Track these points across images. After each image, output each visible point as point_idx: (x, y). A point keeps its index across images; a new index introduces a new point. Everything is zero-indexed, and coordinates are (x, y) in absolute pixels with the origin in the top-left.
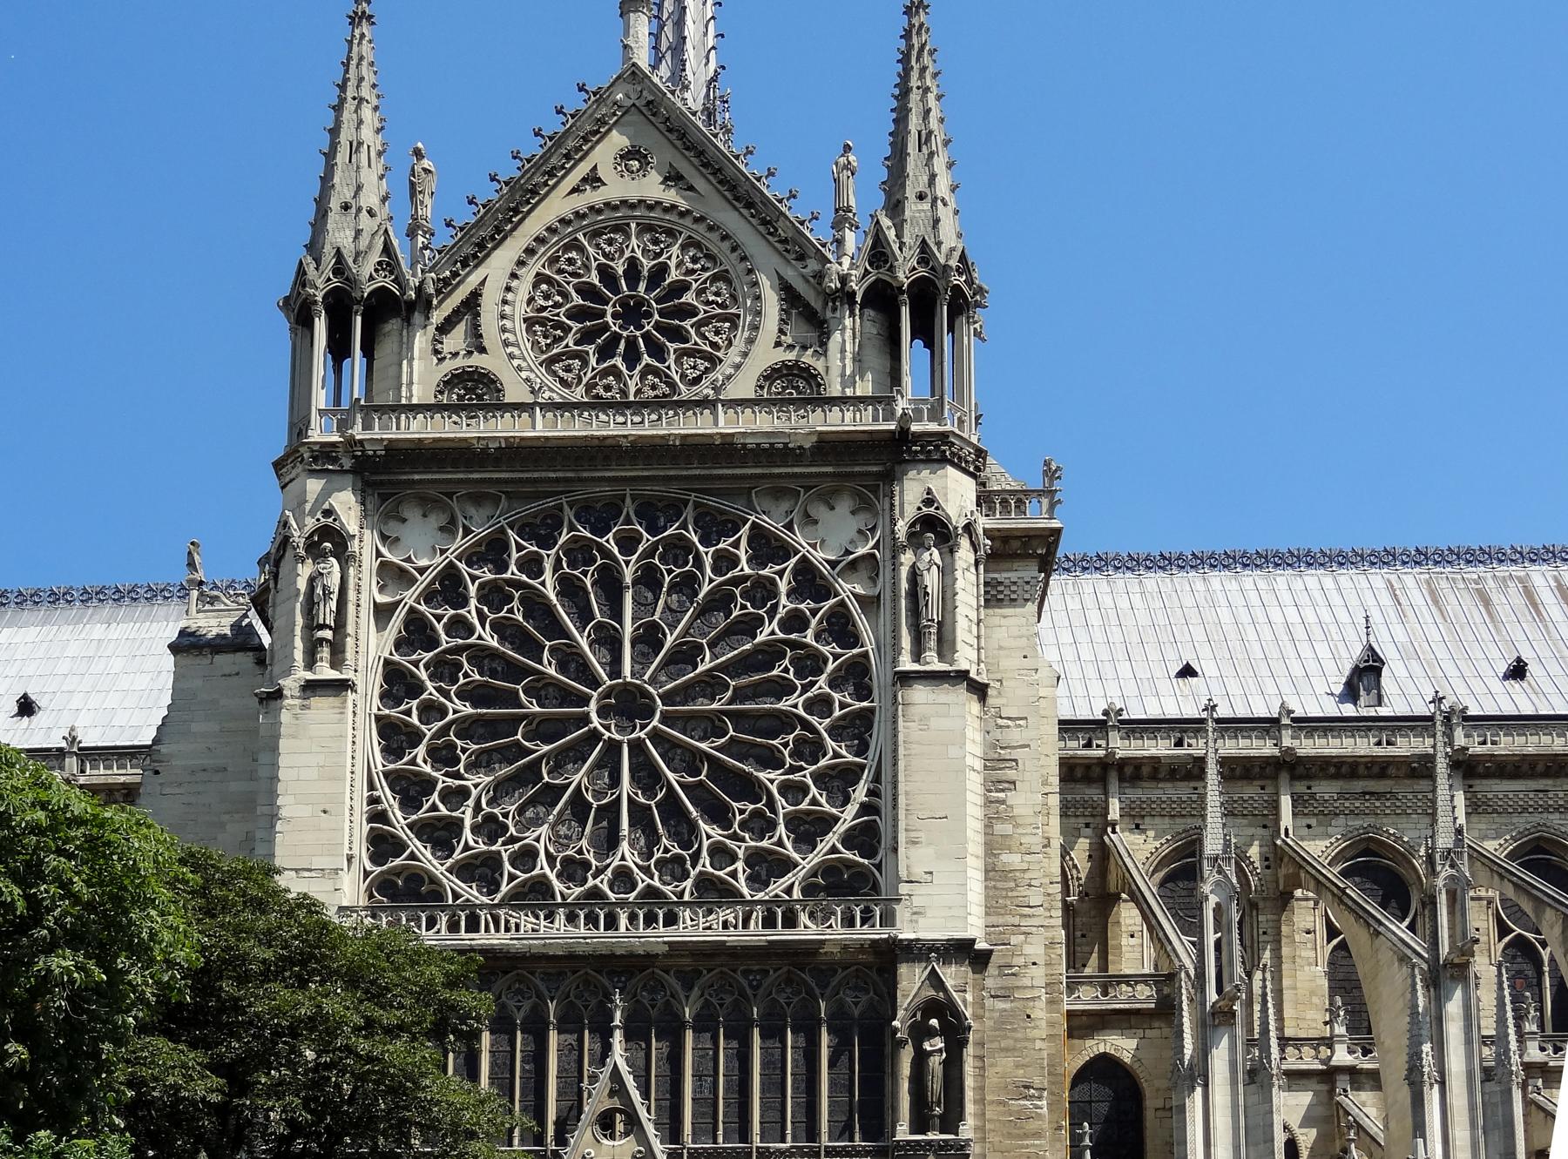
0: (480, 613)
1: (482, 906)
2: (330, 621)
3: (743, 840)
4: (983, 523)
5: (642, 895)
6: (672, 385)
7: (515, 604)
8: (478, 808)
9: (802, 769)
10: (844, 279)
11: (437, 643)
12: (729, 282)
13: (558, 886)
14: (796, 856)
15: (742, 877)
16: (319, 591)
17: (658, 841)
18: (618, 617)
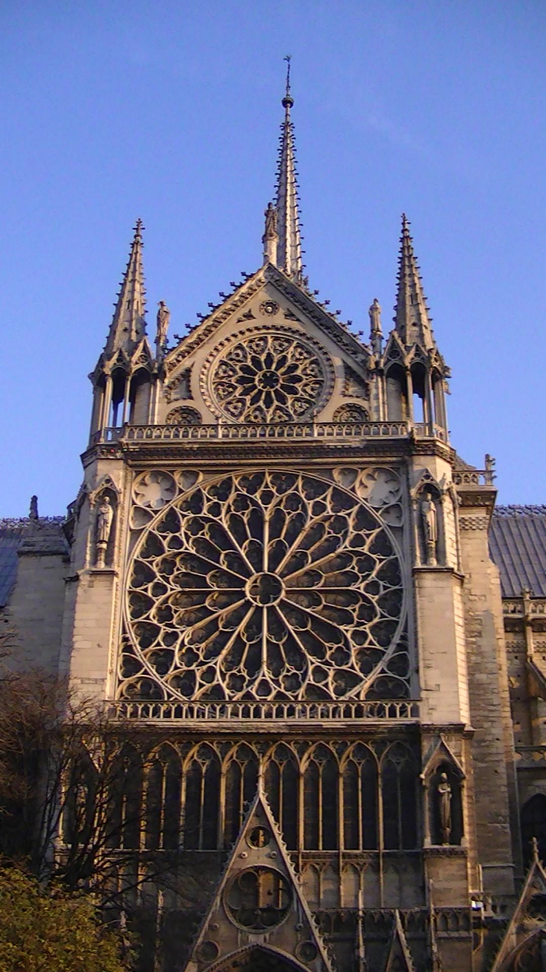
0: (186, 534)
1: (184, 702)
2: (106, 539)
3: (331, 665)
4: (455, 488)
5: (276, 697)
6: (289, 415)
7: (206, 530)
8: (183, 645)
9: (363, 624)
10: (377, 363)
11: (163, 552)
12: (318, 364)
13: (227, 691)
14: (362, 675)
15: (331, 688)
16: (102, 522)
17: (283, 665)
18: (262, 538)
